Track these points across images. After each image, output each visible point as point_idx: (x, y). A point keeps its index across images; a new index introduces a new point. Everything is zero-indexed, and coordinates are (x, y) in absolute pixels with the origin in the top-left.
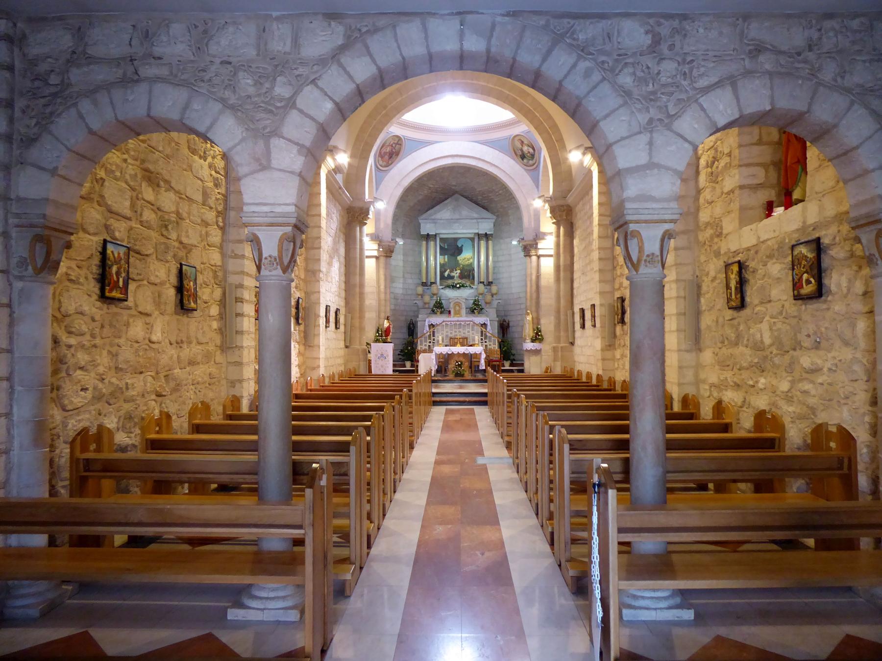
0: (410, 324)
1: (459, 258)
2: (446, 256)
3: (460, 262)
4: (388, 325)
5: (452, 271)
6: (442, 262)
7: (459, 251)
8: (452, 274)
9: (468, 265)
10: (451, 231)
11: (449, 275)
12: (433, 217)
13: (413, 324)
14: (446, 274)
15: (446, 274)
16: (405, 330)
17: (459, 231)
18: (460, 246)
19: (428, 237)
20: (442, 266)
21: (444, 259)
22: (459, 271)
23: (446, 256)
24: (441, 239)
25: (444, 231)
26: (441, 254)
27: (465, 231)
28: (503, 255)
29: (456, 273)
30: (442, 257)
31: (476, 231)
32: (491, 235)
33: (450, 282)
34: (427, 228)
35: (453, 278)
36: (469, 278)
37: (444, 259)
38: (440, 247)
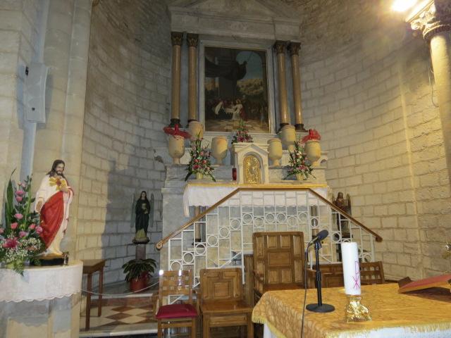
0: (140, 202)
1: (239, 83)
2: (217, 79)
3: (242, 89)
4: (54, 190)
5: (227, 105)
6: (210, 89)
7: (241, 71)
8: (229, 111)
9: (255, 97)
10: (226, 33)
11: (221, 111)
12: (196, 7)
13: (146, 201)
14: (217, 109)
15: (217, 109)
16: (130, 217)
17: (243, 35)
18: (241, 62)
19: (186, 40)
20: (209, 95)
21: (214, 82)
22: (240, 106)
23: (217, 79)
24: (209, 50)
25: (213, 32)
26: (207, 74)
27: (252, 35)
28: (306, 90)
29: (236, 109)
30: (209, 79)
31: (272, 37)
32: (298, 45)
33: (224, 123)
34: (183, 22)
35: (229, 117)
36: (259, 119)
37: (214, 82)
38: (207, 63)
